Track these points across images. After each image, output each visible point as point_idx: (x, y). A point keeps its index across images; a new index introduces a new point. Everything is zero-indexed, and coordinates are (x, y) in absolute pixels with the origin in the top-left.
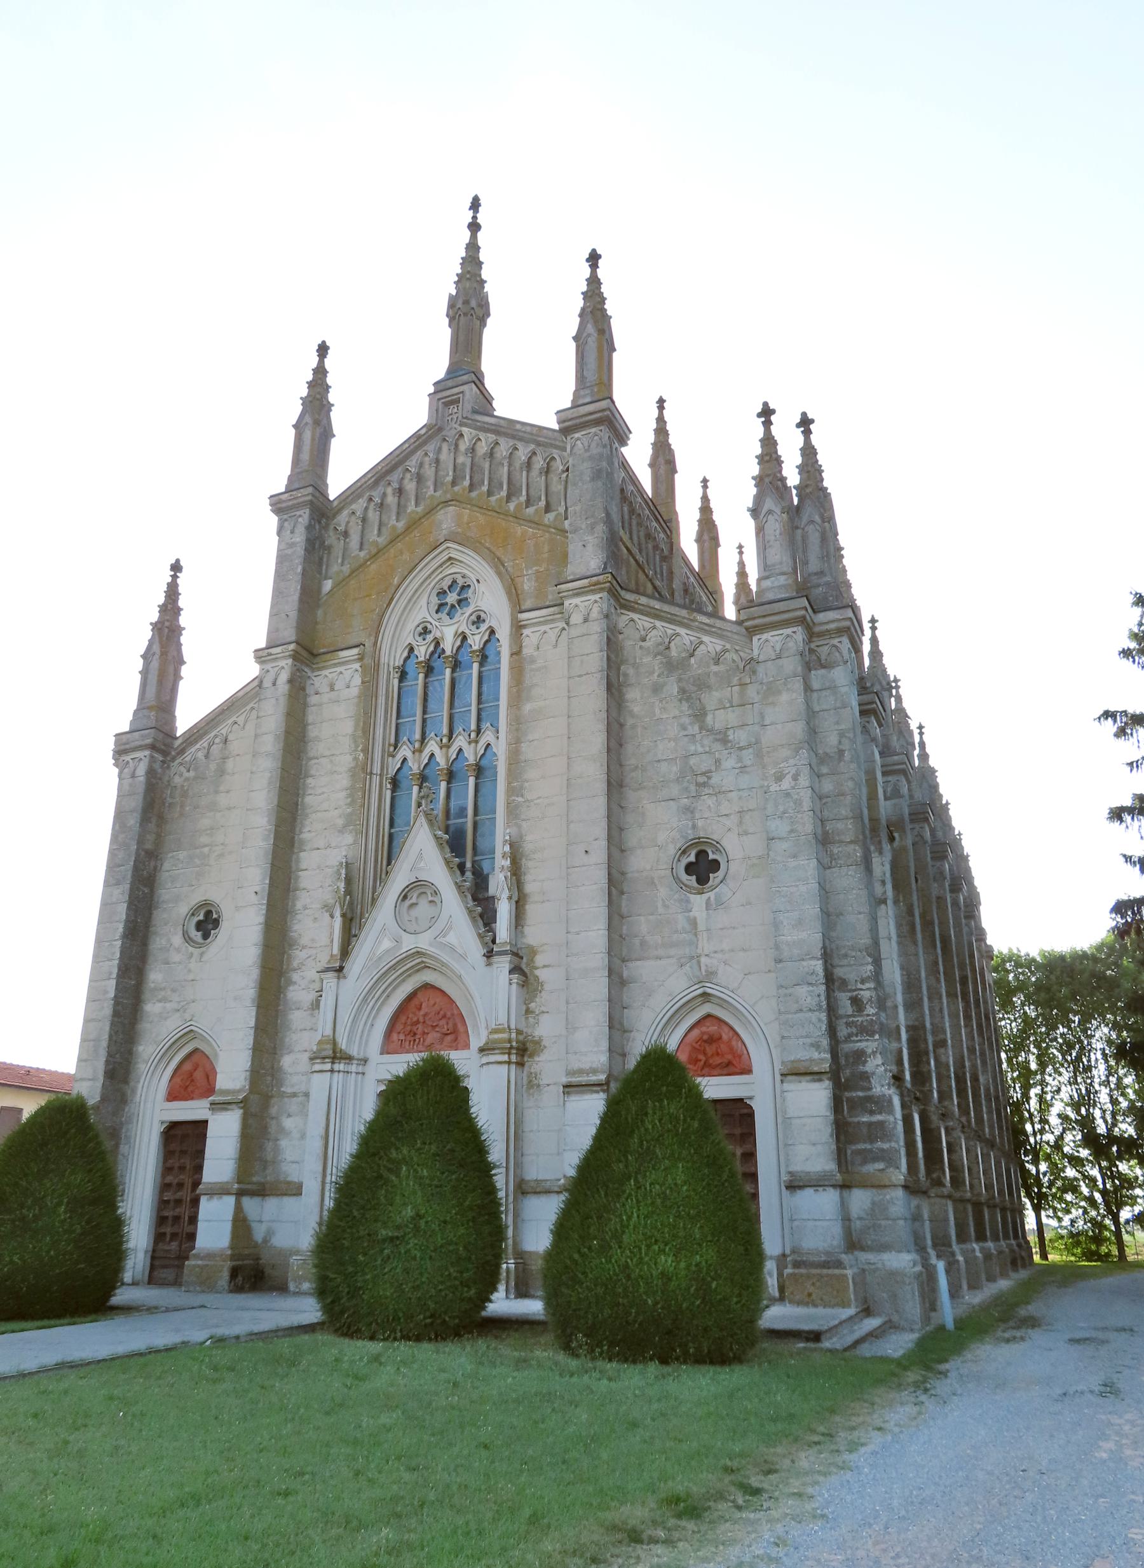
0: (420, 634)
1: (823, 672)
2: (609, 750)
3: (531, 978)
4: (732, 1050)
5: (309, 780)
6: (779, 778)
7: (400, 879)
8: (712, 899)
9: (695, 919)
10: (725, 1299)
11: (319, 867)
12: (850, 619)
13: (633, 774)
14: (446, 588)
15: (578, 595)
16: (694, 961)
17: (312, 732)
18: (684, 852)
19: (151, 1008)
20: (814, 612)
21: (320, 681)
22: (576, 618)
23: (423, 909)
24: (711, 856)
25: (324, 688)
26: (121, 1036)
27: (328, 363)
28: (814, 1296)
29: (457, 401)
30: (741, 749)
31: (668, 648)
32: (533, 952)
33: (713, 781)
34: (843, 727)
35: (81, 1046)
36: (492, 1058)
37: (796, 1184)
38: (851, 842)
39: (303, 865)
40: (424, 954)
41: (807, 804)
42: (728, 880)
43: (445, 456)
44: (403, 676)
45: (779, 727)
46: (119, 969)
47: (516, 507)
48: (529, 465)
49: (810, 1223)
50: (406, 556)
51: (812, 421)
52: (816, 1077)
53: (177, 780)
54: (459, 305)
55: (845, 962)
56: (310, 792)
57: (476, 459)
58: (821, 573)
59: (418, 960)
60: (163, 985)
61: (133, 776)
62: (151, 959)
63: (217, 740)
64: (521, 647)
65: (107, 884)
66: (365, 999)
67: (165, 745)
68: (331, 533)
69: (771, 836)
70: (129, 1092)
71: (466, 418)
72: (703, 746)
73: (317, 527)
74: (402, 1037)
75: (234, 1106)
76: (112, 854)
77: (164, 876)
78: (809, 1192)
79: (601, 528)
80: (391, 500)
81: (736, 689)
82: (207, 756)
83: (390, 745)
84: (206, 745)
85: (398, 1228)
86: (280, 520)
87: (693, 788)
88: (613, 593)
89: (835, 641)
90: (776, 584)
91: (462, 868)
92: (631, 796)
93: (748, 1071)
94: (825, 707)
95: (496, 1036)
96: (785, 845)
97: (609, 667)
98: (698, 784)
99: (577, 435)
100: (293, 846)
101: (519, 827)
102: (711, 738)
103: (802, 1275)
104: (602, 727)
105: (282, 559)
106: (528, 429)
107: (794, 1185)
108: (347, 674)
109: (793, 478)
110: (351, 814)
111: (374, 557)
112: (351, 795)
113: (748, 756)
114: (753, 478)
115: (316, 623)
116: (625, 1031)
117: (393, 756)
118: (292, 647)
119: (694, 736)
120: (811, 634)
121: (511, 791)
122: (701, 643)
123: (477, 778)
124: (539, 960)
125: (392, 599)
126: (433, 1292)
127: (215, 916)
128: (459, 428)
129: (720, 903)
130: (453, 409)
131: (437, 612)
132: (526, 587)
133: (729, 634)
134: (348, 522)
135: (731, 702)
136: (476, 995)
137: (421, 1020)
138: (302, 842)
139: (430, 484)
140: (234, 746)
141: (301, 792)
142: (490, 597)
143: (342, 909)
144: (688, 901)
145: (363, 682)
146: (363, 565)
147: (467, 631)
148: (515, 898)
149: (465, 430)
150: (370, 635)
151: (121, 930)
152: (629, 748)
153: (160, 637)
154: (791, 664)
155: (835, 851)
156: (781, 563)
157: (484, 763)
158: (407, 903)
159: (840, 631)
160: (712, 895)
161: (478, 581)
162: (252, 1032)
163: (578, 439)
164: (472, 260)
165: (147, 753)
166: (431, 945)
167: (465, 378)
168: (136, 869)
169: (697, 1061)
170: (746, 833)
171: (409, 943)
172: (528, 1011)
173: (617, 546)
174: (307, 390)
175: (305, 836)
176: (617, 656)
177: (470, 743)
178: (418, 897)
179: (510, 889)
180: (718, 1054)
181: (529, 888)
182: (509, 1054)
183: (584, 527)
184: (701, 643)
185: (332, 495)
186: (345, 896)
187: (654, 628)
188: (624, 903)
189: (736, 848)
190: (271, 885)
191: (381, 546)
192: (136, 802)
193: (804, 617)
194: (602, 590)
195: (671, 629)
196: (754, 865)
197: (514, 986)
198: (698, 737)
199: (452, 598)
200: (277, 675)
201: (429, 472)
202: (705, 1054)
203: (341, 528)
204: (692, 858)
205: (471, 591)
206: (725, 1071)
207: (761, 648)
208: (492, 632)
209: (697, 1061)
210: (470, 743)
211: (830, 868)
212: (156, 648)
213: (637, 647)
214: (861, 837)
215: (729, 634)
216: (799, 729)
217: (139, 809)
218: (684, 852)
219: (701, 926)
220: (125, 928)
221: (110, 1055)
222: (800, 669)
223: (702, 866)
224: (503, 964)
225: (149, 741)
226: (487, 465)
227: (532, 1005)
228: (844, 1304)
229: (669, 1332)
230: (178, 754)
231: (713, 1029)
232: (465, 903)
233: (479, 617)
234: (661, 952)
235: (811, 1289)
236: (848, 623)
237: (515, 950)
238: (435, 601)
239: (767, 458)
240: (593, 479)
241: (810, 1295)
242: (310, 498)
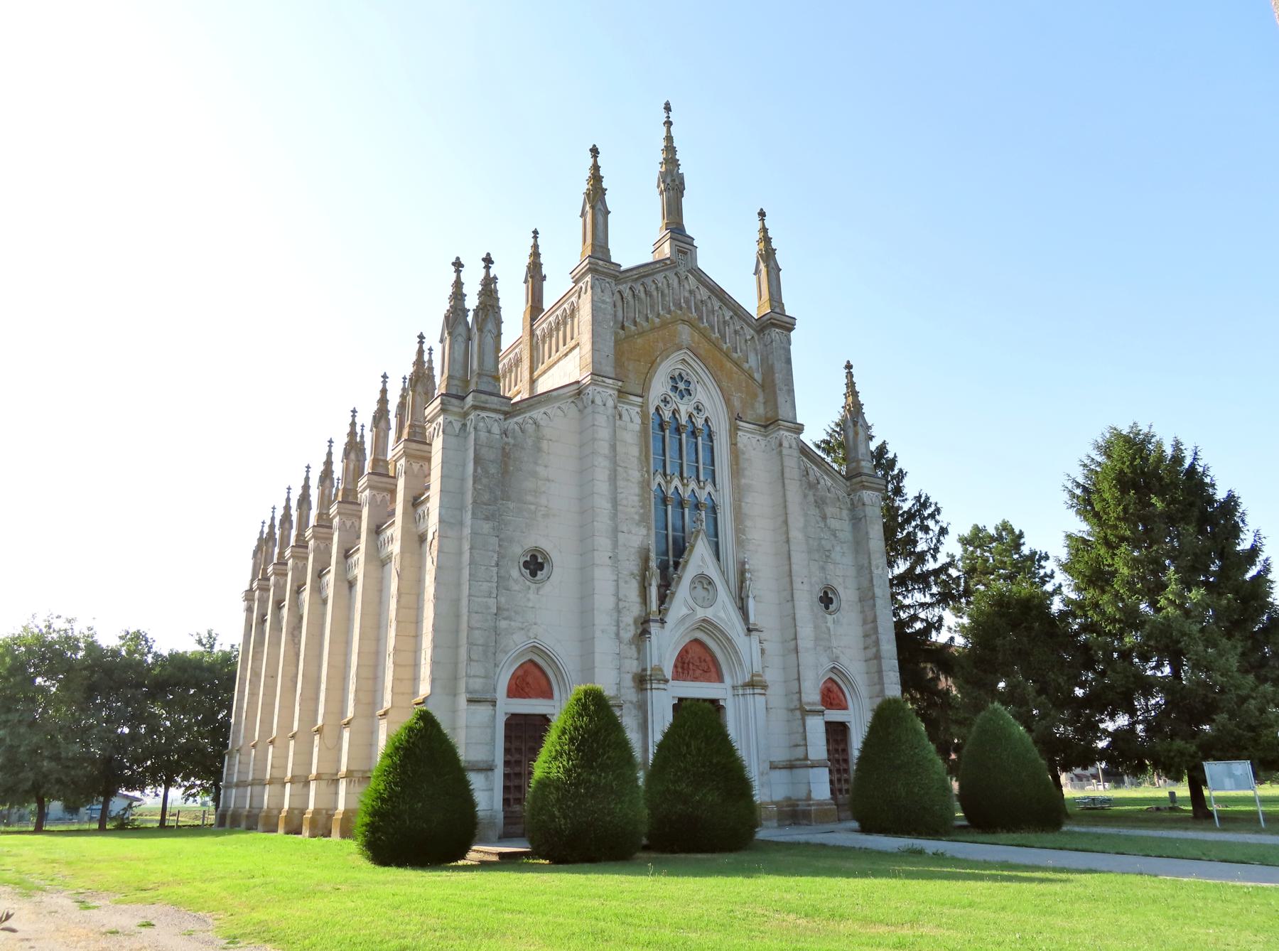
29: (685, 253)
59: (706, 625)
93: (846, 708)
164: (670, 149)
171: (701, 613)
231: (829, 685)
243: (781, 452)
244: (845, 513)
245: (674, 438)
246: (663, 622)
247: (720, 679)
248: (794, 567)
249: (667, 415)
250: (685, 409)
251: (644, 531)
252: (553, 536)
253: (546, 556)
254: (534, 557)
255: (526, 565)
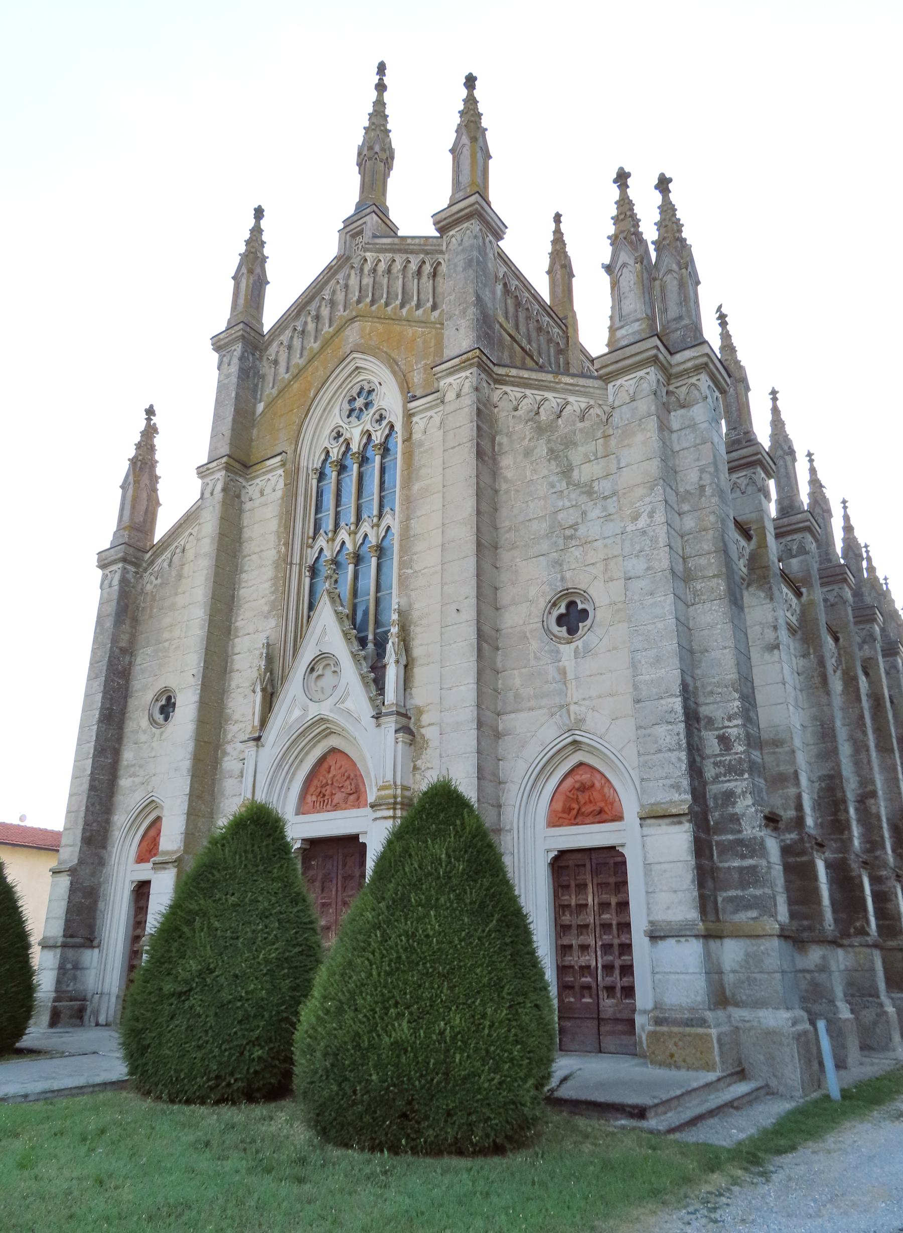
0: (335, 438)
1: (683, 411)
2: (479, 512)
3: (418, 738)
4: (605, 799)
5: (244, 575)
6: (635, 518)
7: (307, 655)
8: (580, 647)
9: (564, 668)
10: (474, 1074)
11: (249, 650)
12: (707, 355)
13: (507, 536)
14: (355, 395)
15: (451, 374)
16: (564, 710)
17: (247, 533)
18: (554, 604)
19: (124, 782)
20: (671, 354)
21: (252, 490)
22: (451, 396)
23: (329, 679)
24: (580, 606)
25: (256, 495)
26: (98, 807)
27: (263, 223)
28: (676, 1058)
30: (605, 498)
31: (537, 413)
32: (419, 711)
33: (578, 534)
34: (703, 462)
35: (66, 817)
36: (380, 814)
37: (657, 934)
38: (714, 576)
39: (237, 650)
40: (328, 720)
41: (662, 540)
42: (595, 628)
43: (353, 281)
44: (321, 476)
45: (635, 467)
46: (95, 750)
47: (408, 311)
48: (419, 272)
49: (672, 977)
50: (320, 372)
51: (670, 180)
52: (675, 820)
53: (149, 588)
54: (365, 152)
55: (710, 700)
56: (243, 585)
57: (377, 279)
58: (680, 318)
59: (321, 727)
60: (133, 763)
61: (110, 586)
62: (125, 741)
63: (178, 551)
64: (411, 434)
65: (90, 679)
66: (279, 765)
67: (136, 558)
68: (265, 363)
69: (628, 576)
70: (107, 855)
71: (368, 243)
72: (570, 501)
73: (251, 359)
74: (314, 798)
75: (170, 865)
76: (94, 651)
77: (137, 669)
78: (671, 942)
79: (472, 311)
80: (311, 326)
81: (601, 441)
82: (170, 565)
83: (308, 538)
84: (169, 556)
85: (186, 982)
86: (220, 356)
87: (561, 541)
88: (481, 366)
89: (693, 380)
90: (630, 331)
91: (363, 642)
92: (505, 557)
93: (619, 818)
94: (685, 445)
95: (383, 793)
96: (642, 583)
97: (479, 435)
98: (566, 538)
99: (451, 233)
100: (230, 633)
101: (409, 596)
102: (578, 491)
103: (663, 1034)
104: (472, 491)
105: (221, 388)
106: (417, 241)
107: (655, 936)
108: (273, 480)
109: (650, 232)
110: (273, 602)
111: (296, 377)
112: (275, 584)
113: (612, 504)
114: (609, 238)
115: (252, 441)
116: (500, 783)
117: (312, 548)
118: (224, 460)
119: (561, 492)
120: (669, 375)
121: (403, 565)
122: (567, 403)
123: (379, 558)
124: (425, 719)
125: (309, 410)
126: (216, 1051)
127: (173, 700)
128: (362, 253)
129: (588, 651)
130: (359, 239)
131: (348, 417)
132: (416, 380)
133: (591, 390)
134: (278, 352)
135: (595, 454)
136: (368, 756)
137: (330, 782)
138: (236, 629)
139: (341, 308)
140: (190, 554)
141: (237, 586)
142: (389, 399)
143: (262, 685)
144: (558, 652)
145: (285, 485)
146: (288, 385)
147: (371, 429)
148: (403, 661)
149: (368, 255)
150: (291, 443)
151: (97, 716)
152: (504, 512)
153: (134, 469)
154: (645, 405)
155: (699, 587)
156: (636, 311)
157: (385, 544)
158: (315, 674)
159: (698, 369)
160: (580, 643)
161: (380, 384)
162: (187, 798)
163: (453, 236)
164: (379, 114)
165: (120, 565)
166: (331, 711)
167: (368, 210)
168: (110, 663)
169: (571, 809)
170: (611, 579)
171: (314, 710)
172: (415, 768)
173: (491, 328)
174: (245, 248)
175: (239, 624)
176: (491, 427)
177: (372, 527)
178: (324, 668)
179: (396, 654)
180: (591, 802)
181: (418, 651)
182: (395, 809)
183: (457, 313)
184: (567, 403)
185: (266, 329)
186: (265, 673)
187: (525, 397)
188: (499, 659)
189: (601, 596)
190: (206, 668)
191: (301, 367)
192: (112, 608)
193: (656, 356)
194: (471, 365)
195: (539, 395)
196: (618, 610)
197: (400, 745)
198: (566, 492)
199: (360, 403)
200: (215, 486)
201: (340, 297)
202: (578, 803)
203: (272, 358)
204: (563, 610)
205: (374, 394)
206: (598, 818)
207: (615, 394)
208: (392, 427)
209: (571, 809)
210: (372, 527)
211: (693, 605)
212: (131, 479)
213: (510, 417)
214: (724, 570)
215: (591, 390)
216: (654, 467)
217: (113, 613)
218: (554, 604)
219: (570, 675)
220: (101, 714)
221: (87, 824)
222: (653, 408)
223: (572, 617)
224: (390, 723)
225: (121, 555)
226: (385, 281)
227: (419, 763)
228: (708, 1067)
229: (404, 1116)
230: (149, 565)
231: (585, 777)
232: (359, 669)
233: (381, 416)
234: (532, 703)
235: (674, 1049)
236: (705, 359)
237: (403, 711)
238: (346, 407)
239: (622, 216)
240: (464, 269)
241: (672, 1056)
242: (241, 333)
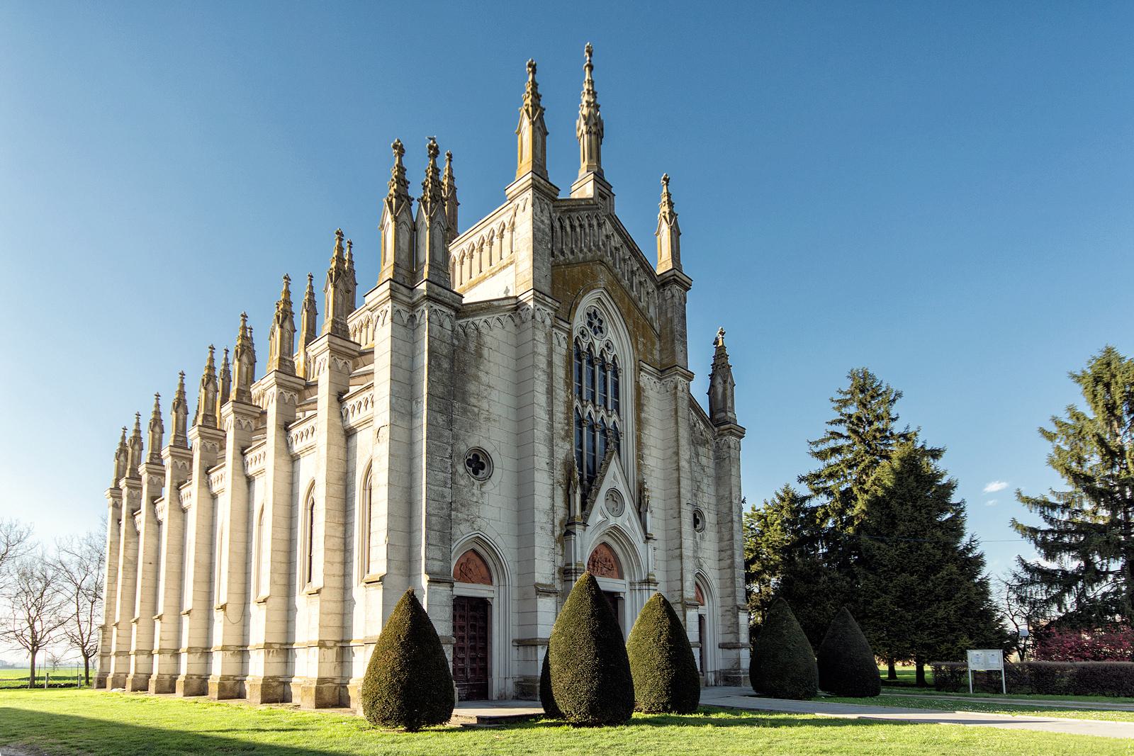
59: (616, 532)
171: (613, 521)
243: (676, 393)
244: (711, 453)
245: (588, 368)
246: (585, 524)
247: (621, 577)
248: (682, 490)
249: (584, 346)
250: (598, 345)
251: (568, 446)
252: (493, 437)
253: (487, 456)
254: (476, 457)
255: (469, 463)
